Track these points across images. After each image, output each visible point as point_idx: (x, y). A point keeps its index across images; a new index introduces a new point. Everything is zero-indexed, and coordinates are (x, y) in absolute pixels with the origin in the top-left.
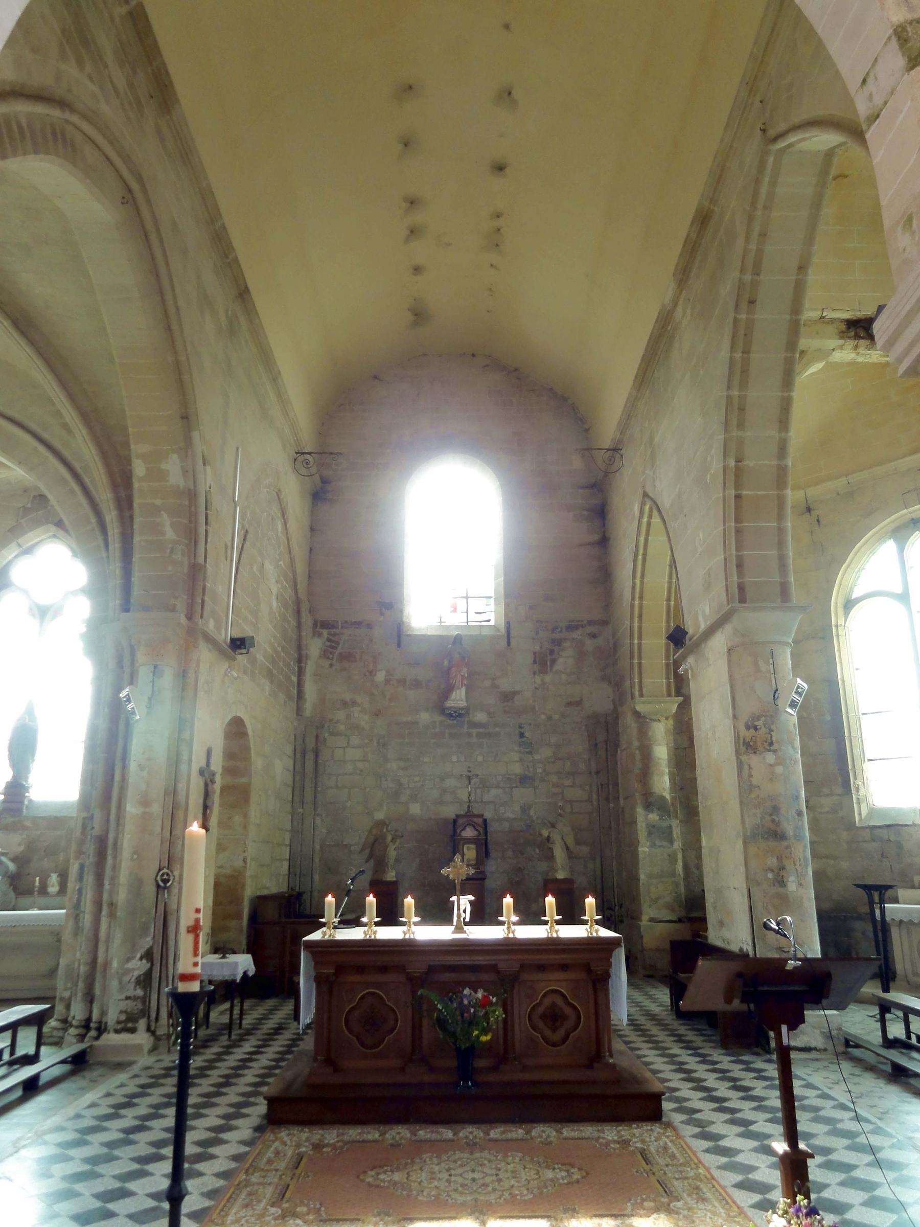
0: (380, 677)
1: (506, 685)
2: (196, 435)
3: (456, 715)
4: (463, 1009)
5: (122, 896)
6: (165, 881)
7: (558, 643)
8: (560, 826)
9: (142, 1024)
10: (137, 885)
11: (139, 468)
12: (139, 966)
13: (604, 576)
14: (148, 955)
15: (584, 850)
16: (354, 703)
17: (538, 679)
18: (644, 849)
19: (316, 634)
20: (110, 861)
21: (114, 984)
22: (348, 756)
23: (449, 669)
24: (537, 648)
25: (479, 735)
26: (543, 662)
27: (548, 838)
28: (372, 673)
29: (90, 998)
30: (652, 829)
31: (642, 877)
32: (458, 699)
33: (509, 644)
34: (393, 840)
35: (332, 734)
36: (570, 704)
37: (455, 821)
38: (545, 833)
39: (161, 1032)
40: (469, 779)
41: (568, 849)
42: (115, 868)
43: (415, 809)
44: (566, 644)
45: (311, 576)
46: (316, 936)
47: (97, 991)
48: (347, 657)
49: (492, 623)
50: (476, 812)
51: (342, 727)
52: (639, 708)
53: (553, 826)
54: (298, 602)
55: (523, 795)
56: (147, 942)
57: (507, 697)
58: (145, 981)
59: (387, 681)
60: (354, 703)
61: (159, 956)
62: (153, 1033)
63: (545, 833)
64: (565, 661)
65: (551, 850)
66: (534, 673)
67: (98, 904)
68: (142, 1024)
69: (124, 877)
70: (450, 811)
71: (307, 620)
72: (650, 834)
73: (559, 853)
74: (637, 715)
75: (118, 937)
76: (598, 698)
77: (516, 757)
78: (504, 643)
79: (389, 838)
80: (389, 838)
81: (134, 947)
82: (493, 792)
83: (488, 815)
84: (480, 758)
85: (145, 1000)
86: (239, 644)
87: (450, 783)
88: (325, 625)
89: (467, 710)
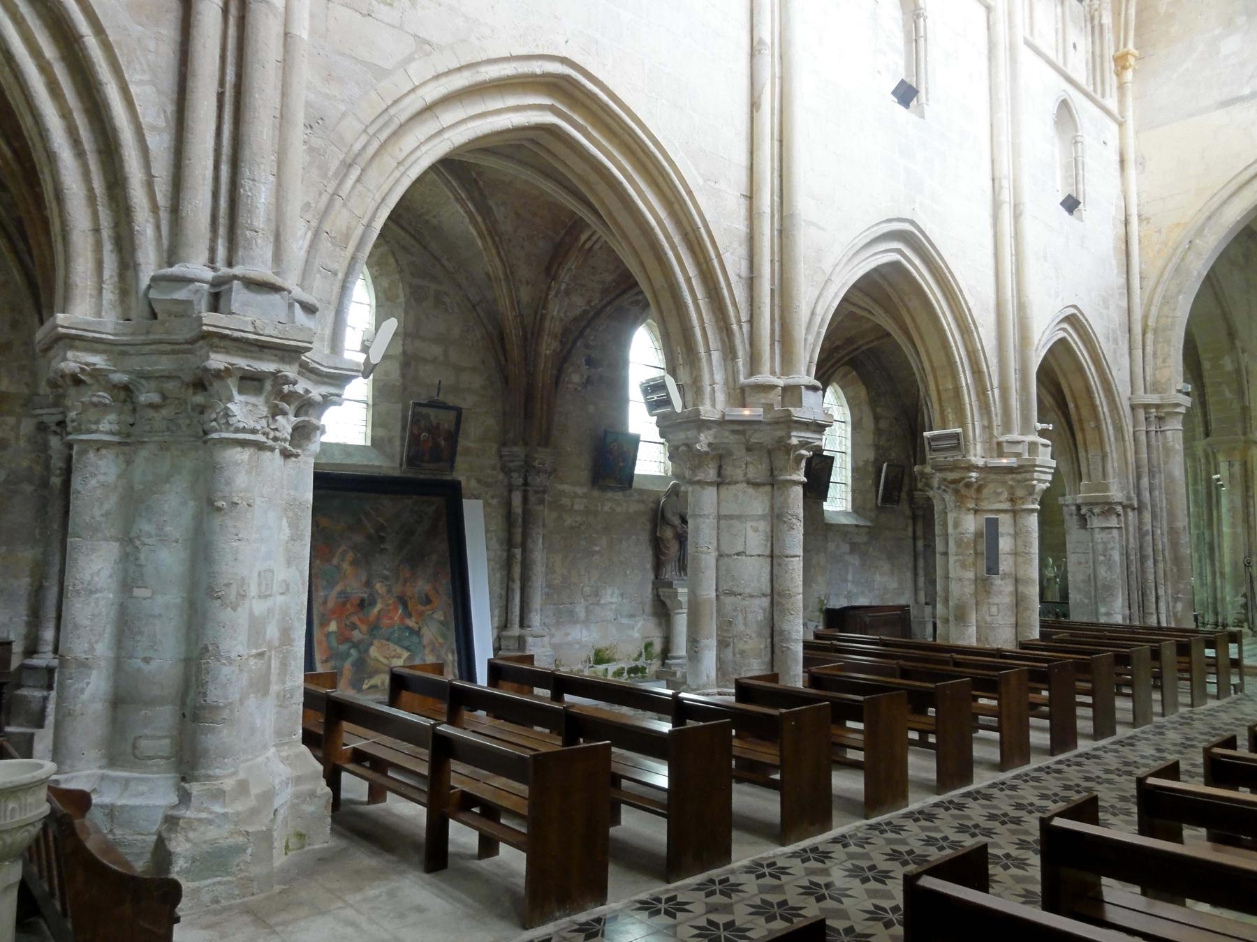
2: (1237, 342)
5: (1228, 569)
9: (1246, 625)
10: (1235, 565)
11: (1206, 365)
12: (1242, 600)
14: (1245, 596)
20: (1217, 554)
21: (1229, 607)
29: (1216, 614)
42: (1221, 556)
47: (1219, 610)
56: (1243, 590)
58: (1245, 606)
67: (1214, 573)
68: (1246, 625)
69: (1227, 560)
75: (1228, 588)
85: (1246, 614)
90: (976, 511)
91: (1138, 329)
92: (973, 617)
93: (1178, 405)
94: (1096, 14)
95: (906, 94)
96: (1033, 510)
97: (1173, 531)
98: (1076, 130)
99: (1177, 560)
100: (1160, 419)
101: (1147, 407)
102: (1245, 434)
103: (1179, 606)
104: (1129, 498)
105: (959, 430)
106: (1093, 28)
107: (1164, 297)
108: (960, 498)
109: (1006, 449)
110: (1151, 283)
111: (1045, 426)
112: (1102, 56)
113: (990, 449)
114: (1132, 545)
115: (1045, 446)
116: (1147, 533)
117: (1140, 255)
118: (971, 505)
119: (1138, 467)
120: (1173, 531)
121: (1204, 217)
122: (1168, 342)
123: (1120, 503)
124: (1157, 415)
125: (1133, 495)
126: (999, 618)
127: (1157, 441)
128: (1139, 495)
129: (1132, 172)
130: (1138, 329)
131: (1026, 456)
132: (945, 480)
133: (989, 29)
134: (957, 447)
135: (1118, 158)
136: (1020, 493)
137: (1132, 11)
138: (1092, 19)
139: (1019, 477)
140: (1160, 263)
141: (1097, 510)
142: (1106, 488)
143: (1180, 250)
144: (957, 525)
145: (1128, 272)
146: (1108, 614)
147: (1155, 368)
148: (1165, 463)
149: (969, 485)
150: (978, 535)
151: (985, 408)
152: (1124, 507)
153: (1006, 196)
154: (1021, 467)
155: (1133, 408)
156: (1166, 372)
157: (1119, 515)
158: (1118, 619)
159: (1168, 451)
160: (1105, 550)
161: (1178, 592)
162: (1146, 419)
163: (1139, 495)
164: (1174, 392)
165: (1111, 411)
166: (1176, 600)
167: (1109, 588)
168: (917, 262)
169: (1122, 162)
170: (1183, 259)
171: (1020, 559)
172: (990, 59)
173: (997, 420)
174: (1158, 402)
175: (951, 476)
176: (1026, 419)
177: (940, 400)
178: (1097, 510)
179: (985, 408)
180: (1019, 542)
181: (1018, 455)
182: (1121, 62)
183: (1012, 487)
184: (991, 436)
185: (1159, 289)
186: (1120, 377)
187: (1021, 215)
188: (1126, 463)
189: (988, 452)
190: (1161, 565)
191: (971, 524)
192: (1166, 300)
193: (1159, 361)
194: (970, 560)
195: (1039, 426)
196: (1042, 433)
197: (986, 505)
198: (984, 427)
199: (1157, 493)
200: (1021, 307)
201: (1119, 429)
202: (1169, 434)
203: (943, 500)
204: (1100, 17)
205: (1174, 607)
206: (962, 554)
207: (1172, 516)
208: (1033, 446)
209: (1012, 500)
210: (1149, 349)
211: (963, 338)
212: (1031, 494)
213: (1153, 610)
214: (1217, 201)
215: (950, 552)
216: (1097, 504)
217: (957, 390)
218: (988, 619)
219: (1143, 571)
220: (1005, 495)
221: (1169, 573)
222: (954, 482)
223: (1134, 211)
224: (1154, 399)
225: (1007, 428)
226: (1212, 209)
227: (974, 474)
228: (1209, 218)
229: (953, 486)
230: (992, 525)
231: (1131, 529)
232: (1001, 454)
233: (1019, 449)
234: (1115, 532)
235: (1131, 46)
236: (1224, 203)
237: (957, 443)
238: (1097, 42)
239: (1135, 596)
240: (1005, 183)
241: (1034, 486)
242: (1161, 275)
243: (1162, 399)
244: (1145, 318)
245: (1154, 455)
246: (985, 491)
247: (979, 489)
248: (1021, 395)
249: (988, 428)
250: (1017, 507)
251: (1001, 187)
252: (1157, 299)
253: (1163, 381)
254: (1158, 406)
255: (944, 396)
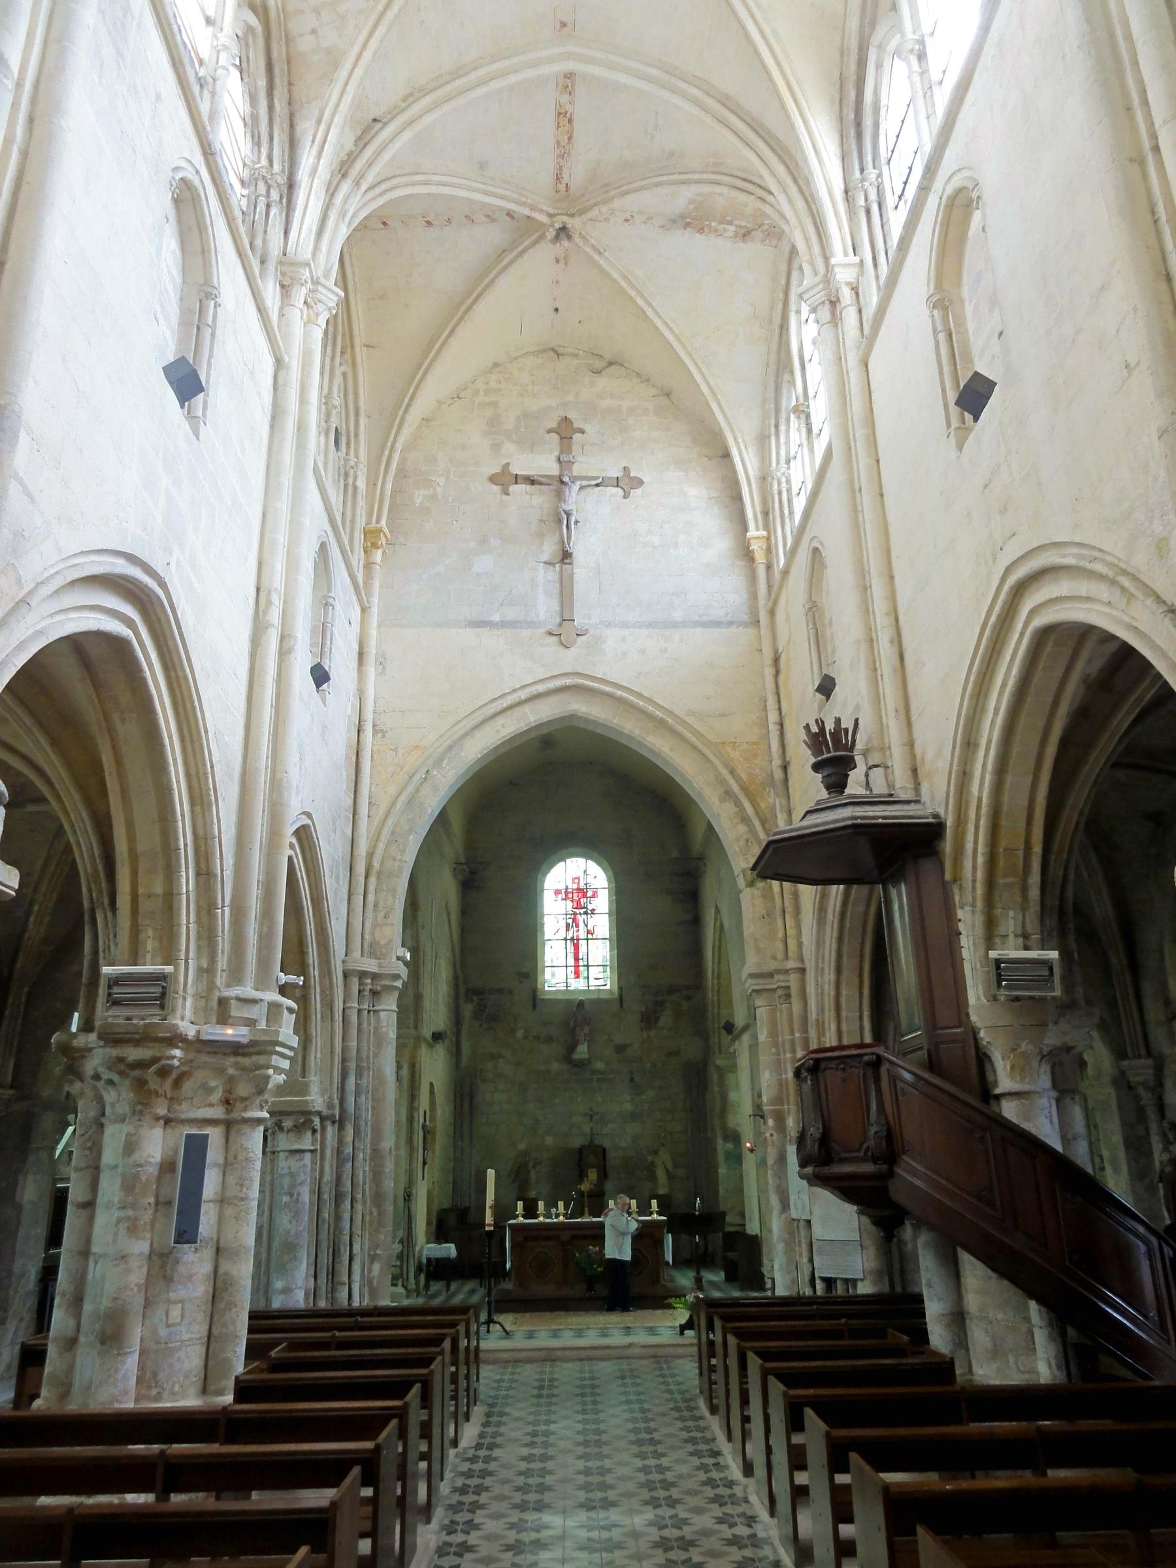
0: (520, 1033)
1: (619, 1039)
3: (581, 1065)
4: (589, 1256)
6: (409, 1196)
7: (661, 1004)
8: (660, 1153)
12: (398, 1248)
13: (695, 950)
14: (401, 1241)
15: (680, 1172)
16: (500, 1056)
17: (645, 1034)
18: (722, 1171)
19: (469, 999)
22: (496, 1099)
23: (574, 1029)
24: (643, 1009)
25: (598, 1080)
26: (649, 1020)
27: (652, 1163)
28: (513, 1031)
30: (729, 1155)
31: (721, 1191)
32: (582, 1051)
33: (621, 1005)
34: (534, 1166)
35: (483, 1080)
36: (669, 1055)
37: (581, 1151)
38: (650, 1158)
39: (409, 1287)
40: (591, 1116)
41: (668, 1171)
43: (549, 1140)
44: (668, 1005)
45: (462, 950)
46: (511, 1222)
48: (494, 1018)
49: (608, 987)
50: (597, 1143)
51: (490, 1076)
52: (718, 1062)
53: (656, 1153)
54: (456, 978)
55: (633, 1128)
57: (620, 1049)
58: (400, 1257)
59: (525, 1038)
60: (500, 1056)
61: (408, 1240)
62: (406, 1288)
63: (650, 1158)
64: (666, 1019)
65: (654, 1171)
66: (642, 1029)
70: (576, 1142)
71: (462, 989)
72: (726, 1159)
73: (661, 1174)
74: (717, 1067)
76: (691, 1049)
77: (628, 1098)
78: (616, 1006)
79: (531, 1164)
80: (531, 1164)
81: (394, 1238)
82: (610, 1126)
83: (606, 1144)
84: (600, 1099)
85: (401, 1267)
86: (437, 1037)
87: (577, 1119)
88: (477, 992)
89: (589, 1060)
90: (168, 1121)
91: (361, 868)
92: (136, 1334)
93: (397, 977)
94: (352, 472)
95: (186, 382)
96: (259, 1121)
97: (376, 1155)
98: (329, 590)
99: (378, 1198)
100: (374, 993)
101: (362, 975)
102: (416, 1027)
103: (376, 1267)
104: (330, 1106)
105: (169, 969)
106: (346, 486)
107: (393, 833)
108: (143, 1095)
109: (235, 1011)
110: (380, 812)
111: (292, 978)
112: (353, 522)
113: (206, 1010)
114: (327, 1177)
115: (290, 1010)
116: (345, 1160)
117: (371, 776)
118: (162, 1111)
119: (344, 1060)
120: (376, 1155)
121: (445, 745)
122: (394, 891)
123: (319, 1113)
124: (371, 986)
125: (336, 1102)
126: (183, 1329)
127: (369, 1024)
128: (342, 1100)
129: (371, 670)
130: (361, 868)
131: (262, 1025)
132: (121, 1060)
133: (275, 388)
134: (162, 1000)
135: (356, 647)
136: (243, 1089)
137: (389, 486)
138: (346, 475)
139: (246, 1061)
140: (392, 790)
141: (288, 1123)
142: (304, 1090)
143: (417, 778)
144: (130, 1147)
145: (355, 792)
146: (286, 1291)
147: (375, 925)
148: (375, 1056)
149: (164, 1072)
150: (167, 1167)
151: (208, 935)
152: (323, 1119)
153: (275, 616)
154: (253, 1043)
155: (346, 975)
156: (388, 931)
157: (314, 1131)
158: (299, 1300)
159: (380, 1040)
160: (293, 1186)
161: (377, 1246)
162: (360, 991)
163: (342, 1100)
164: (394, 959)
165: (322, 976)
166: (373, 1258)
167: (290, 1248)
168: (154, 656)
169: (361, 655)
170: (417, 791)
171: (229, 1211)
172: (272, 427)
173: (222, 962)
174: (375, 970)
175: (134, 1054)
176: (264, 963)
177: (135, 911)
178: (288, 1123)
179: (208, 935)
180: (231, 1180)
181: (251, 1023)
182: (372, 538)
183: (231, 1080)
184: (211, 986)
185: (390, 822)
186: (337, 929)
187: (290, 651)
188: (332, 1052)
189: (202, 1014)
190: (359, 1207)
191: (156, 1145)
192: (394, 837)
193: (381, 915)
194: (147, 1216)
195: (283, 978)
196: (284, 990)
197: (187, 1111)
198: (200, 971)
199: (363, 1098)
200: (276, 785)
201: (329, 1005)
202: (382, 1014)
203: (100, 1100)
204: (356, 477)
205: (370, 1270)
206: (134, 1206)
207: (377, 1131)
208: (274, 1007)
209: (227, 1102)
210: (371, 897)
211: (192, 812)
212: (261, 1091)
213: (346, 1279)
214: (460, 730)
215: (101, 1200)
216: (289, 1114)
217: (170, 897)
218: (163, 1332)
219: (338, 1217)
220: (217, 1096)
221: (367, 1218)
222: (141, 1065)
223: (369, 717)
224: (371, 965)
225: (236, 976)
226: (455, 737)
227: (177, 1053)
228: (450, 748)
229: (137, 1073)
230: (196, 1148)
231: (328, 1153)
232: (224, 1019)
233: (253, 1012)
234: (308, 1156)
235: (383, 523)
236: (466, 734)
237: (160, 992)
238: (349, 504)
239: (325, 1258)
240: (275, 598)
241: (269, 1077)
242: (393, 805)
243: (380, 965)
244: (370, 855)
245: (365, 1044)
246: (188, 1086)
247: (177, 1084)
248: (261, 924)
249: (207, 972)
250: (235, 1115)
251: (269, 603)
252: (386, 832)
253: (383, 942)
254: (375, 976)
255: (145, 906)
